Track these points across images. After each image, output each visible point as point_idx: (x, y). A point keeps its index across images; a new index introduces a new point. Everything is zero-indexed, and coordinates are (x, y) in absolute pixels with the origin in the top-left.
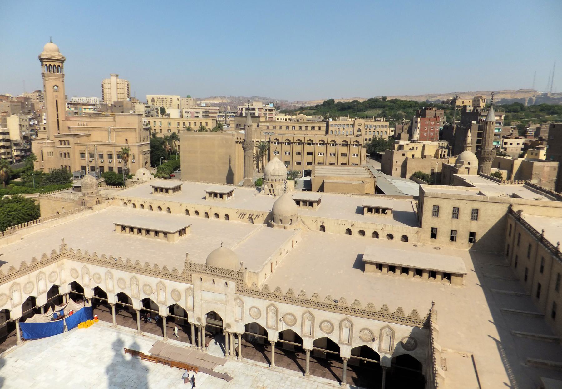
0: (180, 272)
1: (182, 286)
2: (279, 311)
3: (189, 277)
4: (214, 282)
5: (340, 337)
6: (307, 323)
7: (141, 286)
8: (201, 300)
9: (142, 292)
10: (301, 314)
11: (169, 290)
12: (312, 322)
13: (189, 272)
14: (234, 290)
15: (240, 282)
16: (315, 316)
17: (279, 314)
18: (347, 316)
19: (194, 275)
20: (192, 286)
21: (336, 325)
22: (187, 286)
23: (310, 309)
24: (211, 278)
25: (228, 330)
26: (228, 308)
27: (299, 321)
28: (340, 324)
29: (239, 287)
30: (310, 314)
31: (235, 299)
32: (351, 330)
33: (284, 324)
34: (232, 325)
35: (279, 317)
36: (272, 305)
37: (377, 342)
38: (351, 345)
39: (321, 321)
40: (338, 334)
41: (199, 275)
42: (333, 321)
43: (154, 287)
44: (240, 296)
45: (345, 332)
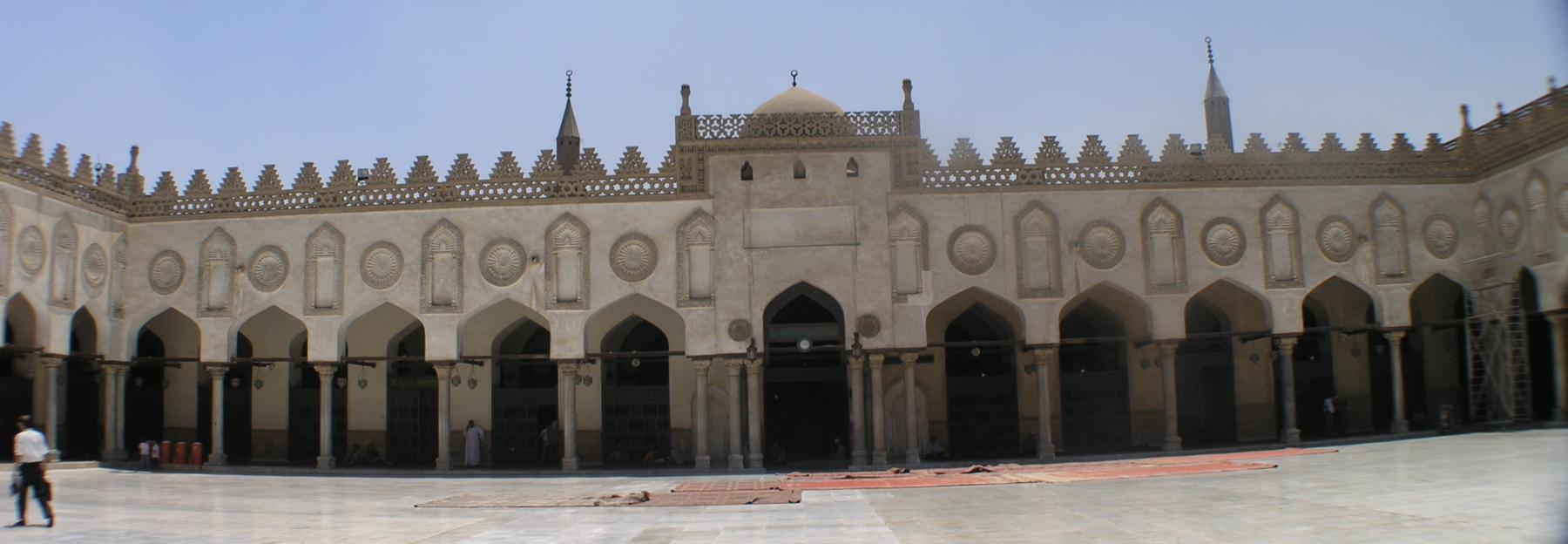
0: (654, 160)
1: (660, 217)
3: (694, 173)
4: (800, 175)
6: (1162, 241)
7: (472, 255)
8: (749, 248)
9: (474, 280)
10: (1137, 214)
11: (602, 243)
12: (1179, 234)
16: (1184, 212)
17: (1061, 235)
19: (713, 161)
20: (707, 205)
21: (1251, 225)
22: (686, 206)
23: (1164, 192)
25: (868, 343)
26: (864, 255)
27: (1134, 244)
28: (1263, 221)
33: (1084, 267)
34: (885, 319)
35: (1063, 245)
37: (1365, 250)
40: (1260, 254)
41: (739, 159)
42: (1239, 217)
43: (534, 244)
44: (909, 198)
45: (1280, 241)
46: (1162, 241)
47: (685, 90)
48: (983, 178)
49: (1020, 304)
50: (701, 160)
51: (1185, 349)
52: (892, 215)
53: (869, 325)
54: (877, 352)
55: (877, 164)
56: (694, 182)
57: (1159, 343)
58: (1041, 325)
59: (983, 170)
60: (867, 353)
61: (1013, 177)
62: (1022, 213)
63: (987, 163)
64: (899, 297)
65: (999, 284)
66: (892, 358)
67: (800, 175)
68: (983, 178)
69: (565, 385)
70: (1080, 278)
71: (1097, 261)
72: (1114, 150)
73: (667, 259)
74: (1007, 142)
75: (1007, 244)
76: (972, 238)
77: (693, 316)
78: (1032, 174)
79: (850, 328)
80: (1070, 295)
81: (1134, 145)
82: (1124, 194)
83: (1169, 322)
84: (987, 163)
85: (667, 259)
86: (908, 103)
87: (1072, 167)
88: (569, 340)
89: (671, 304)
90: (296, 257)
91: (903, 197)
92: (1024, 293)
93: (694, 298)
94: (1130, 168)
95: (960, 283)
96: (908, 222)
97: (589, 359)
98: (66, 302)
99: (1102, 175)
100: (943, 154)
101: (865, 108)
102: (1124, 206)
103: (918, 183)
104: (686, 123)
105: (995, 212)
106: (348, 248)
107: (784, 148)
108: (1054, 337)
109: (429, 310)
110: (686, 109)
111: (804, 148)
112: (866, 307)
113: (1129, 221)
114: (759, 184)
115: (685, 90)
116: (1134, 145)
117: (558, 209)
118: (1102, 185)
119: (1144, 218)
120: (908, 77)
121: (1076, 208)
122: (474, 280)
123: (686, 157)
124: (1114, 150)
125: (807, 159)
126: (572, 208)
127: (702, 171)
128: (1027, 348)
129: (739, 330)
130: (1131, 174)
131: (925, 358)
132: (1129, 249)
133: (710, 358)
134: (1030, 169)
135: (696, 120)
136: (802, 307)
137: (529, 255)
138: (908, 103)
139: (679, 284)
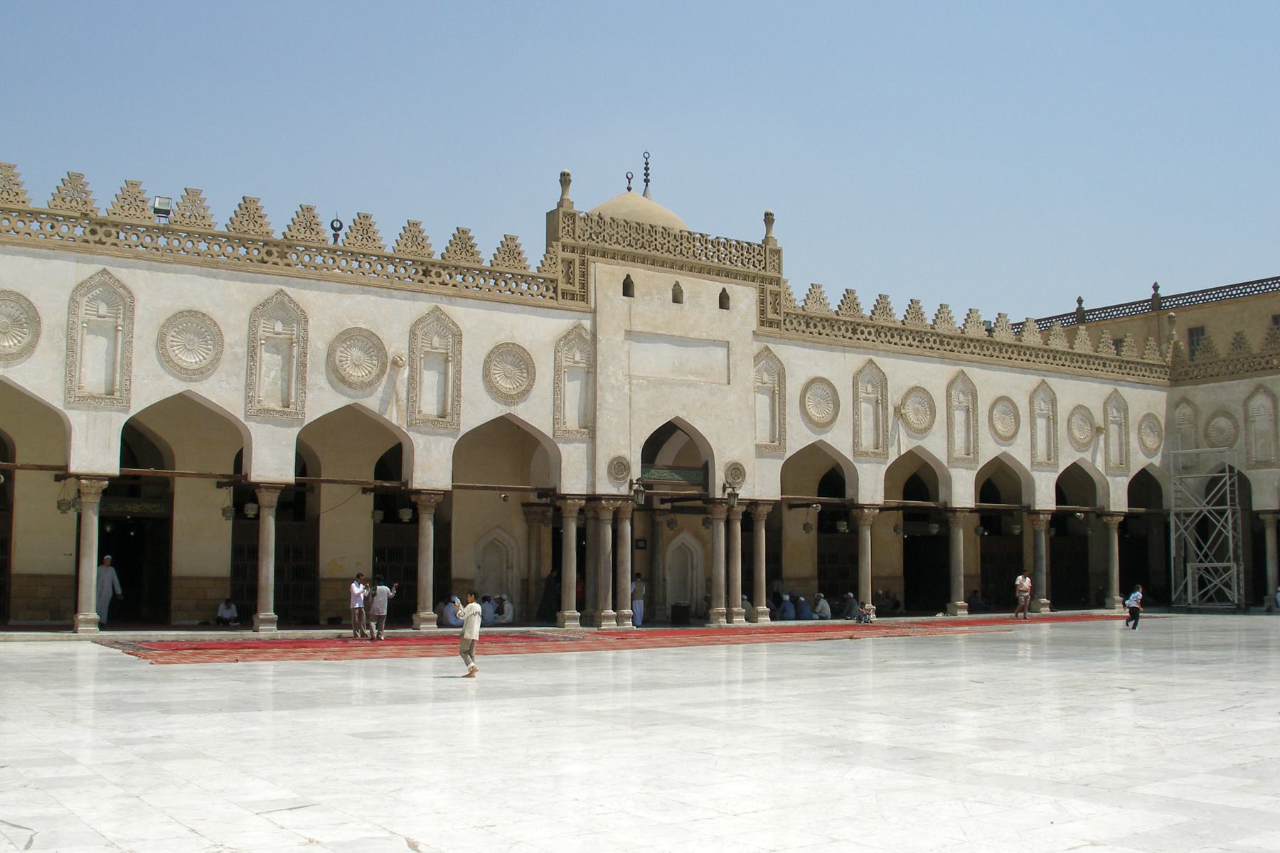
4: (677, 298)
9: (317, 377)
13: (576, 257)
14: (753, 322)
15: (770, 287)
31: (757, 358)
32: (1052, 420)
38: (1056, 465)
41: (620, 270)
47: (565, 179)
53: (736, 471)
67: (677, 298)
90: (53, 313)
108: (1052, 506)
114: (639, 302)
115: (565, 179)
120: (770, 211)
122: (317, 377)
123: (568, 255)
135: (572, 216)
136: (671, 443)
137: (391, 351)
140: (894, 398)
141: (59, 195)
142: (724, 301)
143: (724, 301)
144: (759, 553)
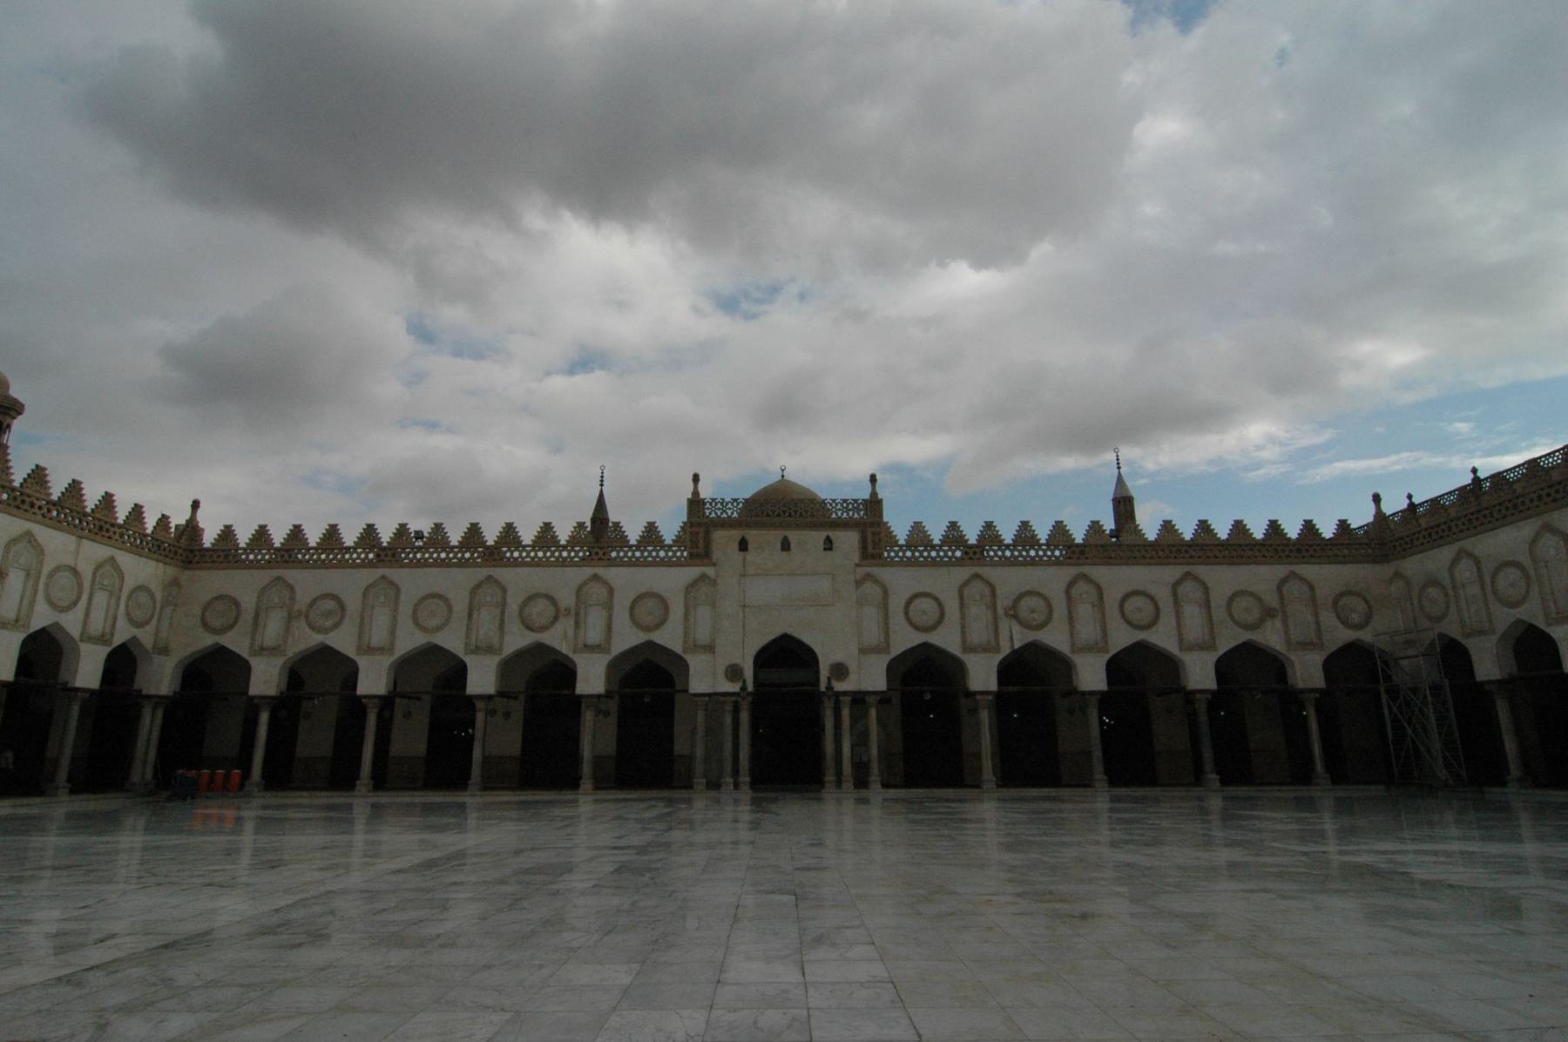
0: (670, 530)
1: (672, 581)
2: (998, 592)
3: (701, 545)
4: (786, 546)
5: (1180, 634)
6: (1084, 611)
15: (870, 530)
18: (1187, 568)
19: (719, 536)
20: (710, 571)
22: (692, 572)
23: (1086, 569)
24: (775, 536)
25: (840, 686)
27: (1060, 610)
28: (1175, 594)
29: (870, 546)
30: (1090, 581)
31: (858, 583)
33: (1016, 628)
34: (852, 666)
35: (1000, 611)
36: (977, 576)
39: (1119, 596)
41: (736, 534)
43: (567, 599)
46: (1084, 611)
47: (696, 478)
48: (934, 554)
49: (965, 658)
50: (707, 533)
51: (1105, 701)
52: (859, 583)
53: (840, 671)
54: (845, 693)
55: (848, 541)
56: (702, 550)
57: (1083, 693)
58: (982, 676)
59: (933, 547)
60: (838, 694)
61: (958, 554)
62: (966, 584)
63: (937, 541)
64: (863, 651)
65: (947, 639)
66: (859, 699)
67: (786, 546)
68: (934, 554)
69: (588, 716)
70: (1015, 637)
71: (1027, 626)
72: (1043, 534)
73: (677, 612)
74: (953, 526)
75: (952, 607)
76: (925, 604)
77: (696, 663)
78: (974, 552)
79: (824, 673)
80: (1006, 650)
81: (1059, 529)
82: (1053, 569)
83: (1091, 676)
84: (937, 541)
85: (677, 612)
86: (874, 494)
87: (1007, 546)
88: (592, 679)
89: (678, 649)
91: (868, 569)
92: (967, 648)
93: (697, 648)
94: (1057, 547)
95: (917, 639)
96: (871, 589)
97: (608, 694)
98: (102, 640)
99: (1032, 553)
100: (901, 532)
101: (839, 497)
102: (1053, 580)
103: (880, 556)
104: (696, 503)
105: (945, 583)
106: (402, 597)
107: (773, 526)
109: (473, 652)
110: (696, 493)
111: (788, 526)
112: (838, 657)
113: (1057, 595)
115: (696, 478)
116: (1059, 529)
117: (588, 572)
118: (1033, 562)
119: (1068, 592)
121: (1009, 581)
124: (1043, 534)
125: (793, 536)
126: (600, 571)
127: (708, 545)
128: (970, 695)
129: (734, 672)
130: (1057, 553)
131: (883, 699)
132: (1055, 615)
133: (709, 695)
134: (972, 546)
135: (703, 502)
136: (786, 656)
137: (562, 605)
138: (874, 494)
139: (686, 634)
140: (1003, 603)
141: (362, 538)
142: (829, 545)
143: (829, 545)
144: (992, 735)
